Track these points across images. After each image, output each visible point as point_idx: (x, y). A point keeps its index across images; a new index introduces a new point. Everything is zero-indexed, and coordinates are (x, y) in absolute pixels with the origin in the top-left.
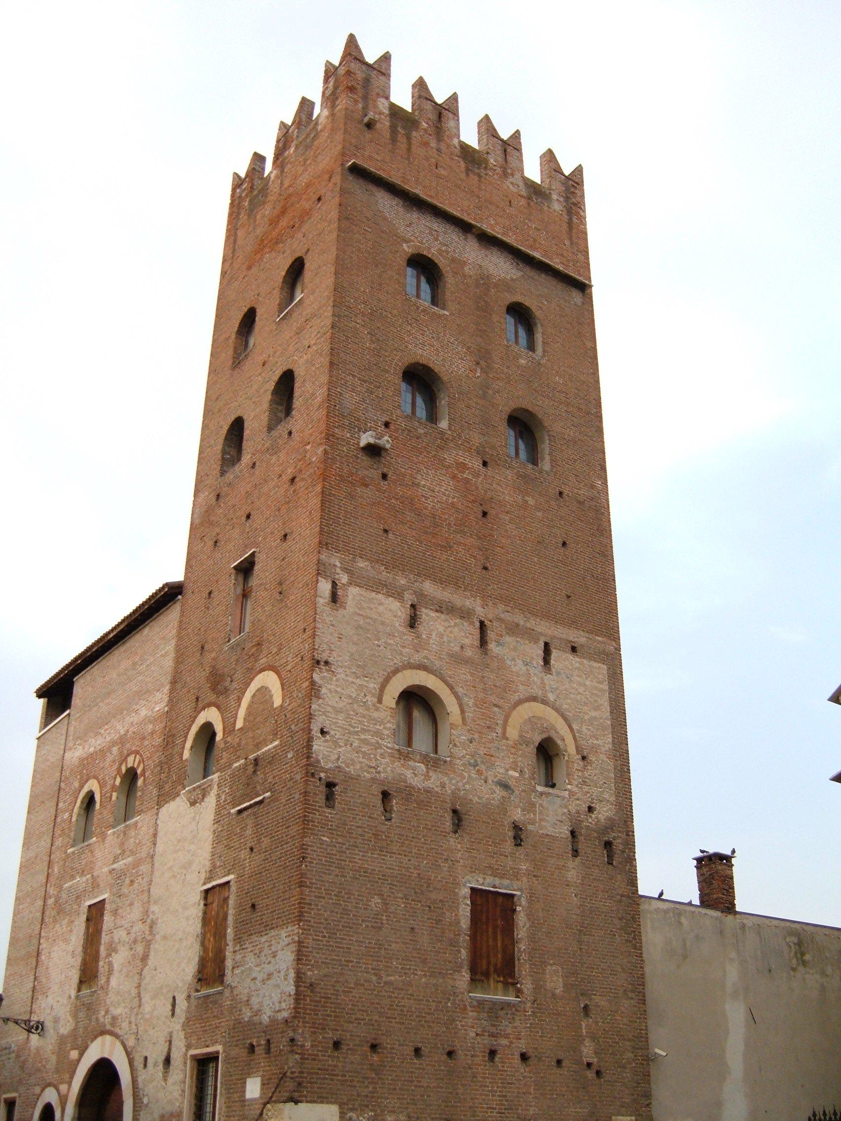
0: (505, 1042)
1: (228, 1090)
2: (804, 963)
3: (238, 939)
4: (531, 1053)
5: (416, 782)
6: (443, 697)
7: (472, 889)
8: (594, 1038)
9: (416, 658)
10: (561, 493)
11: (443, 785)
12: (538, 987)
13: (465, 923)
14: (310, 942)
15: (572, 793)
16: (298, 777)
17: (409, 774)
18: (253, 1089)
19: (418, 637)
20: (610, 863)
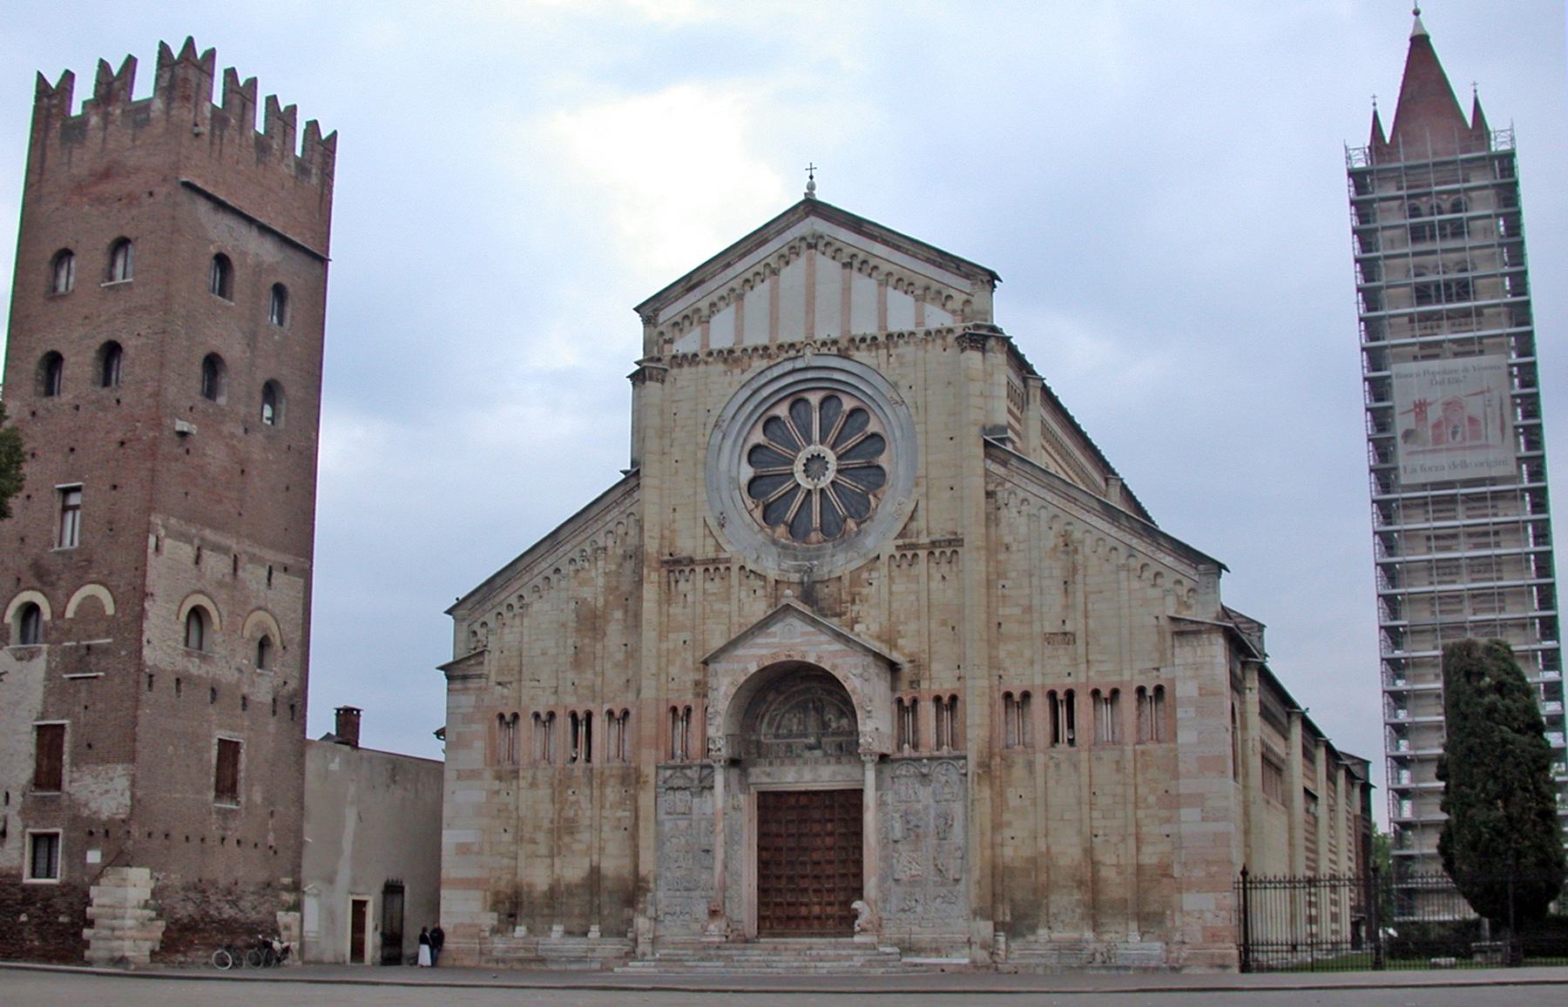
0: (229, 833)
1: (68, 853)
2: (395, 782)
3: (74, 763)
4: (243, 840)
5: (194, 671)
6: (209, 608)
7: (220, 740)
8: (275, 831)
9: (199, 586)
10: (289, 447)
11: (208, 673)
12: (249, 799)
13: (214, 761)
14: (139, 775)
15: (275, 673)
16: (132, 670)
17: (190, 666)
18: (94, 857)
19: (200, 570)
20: (292, 719)
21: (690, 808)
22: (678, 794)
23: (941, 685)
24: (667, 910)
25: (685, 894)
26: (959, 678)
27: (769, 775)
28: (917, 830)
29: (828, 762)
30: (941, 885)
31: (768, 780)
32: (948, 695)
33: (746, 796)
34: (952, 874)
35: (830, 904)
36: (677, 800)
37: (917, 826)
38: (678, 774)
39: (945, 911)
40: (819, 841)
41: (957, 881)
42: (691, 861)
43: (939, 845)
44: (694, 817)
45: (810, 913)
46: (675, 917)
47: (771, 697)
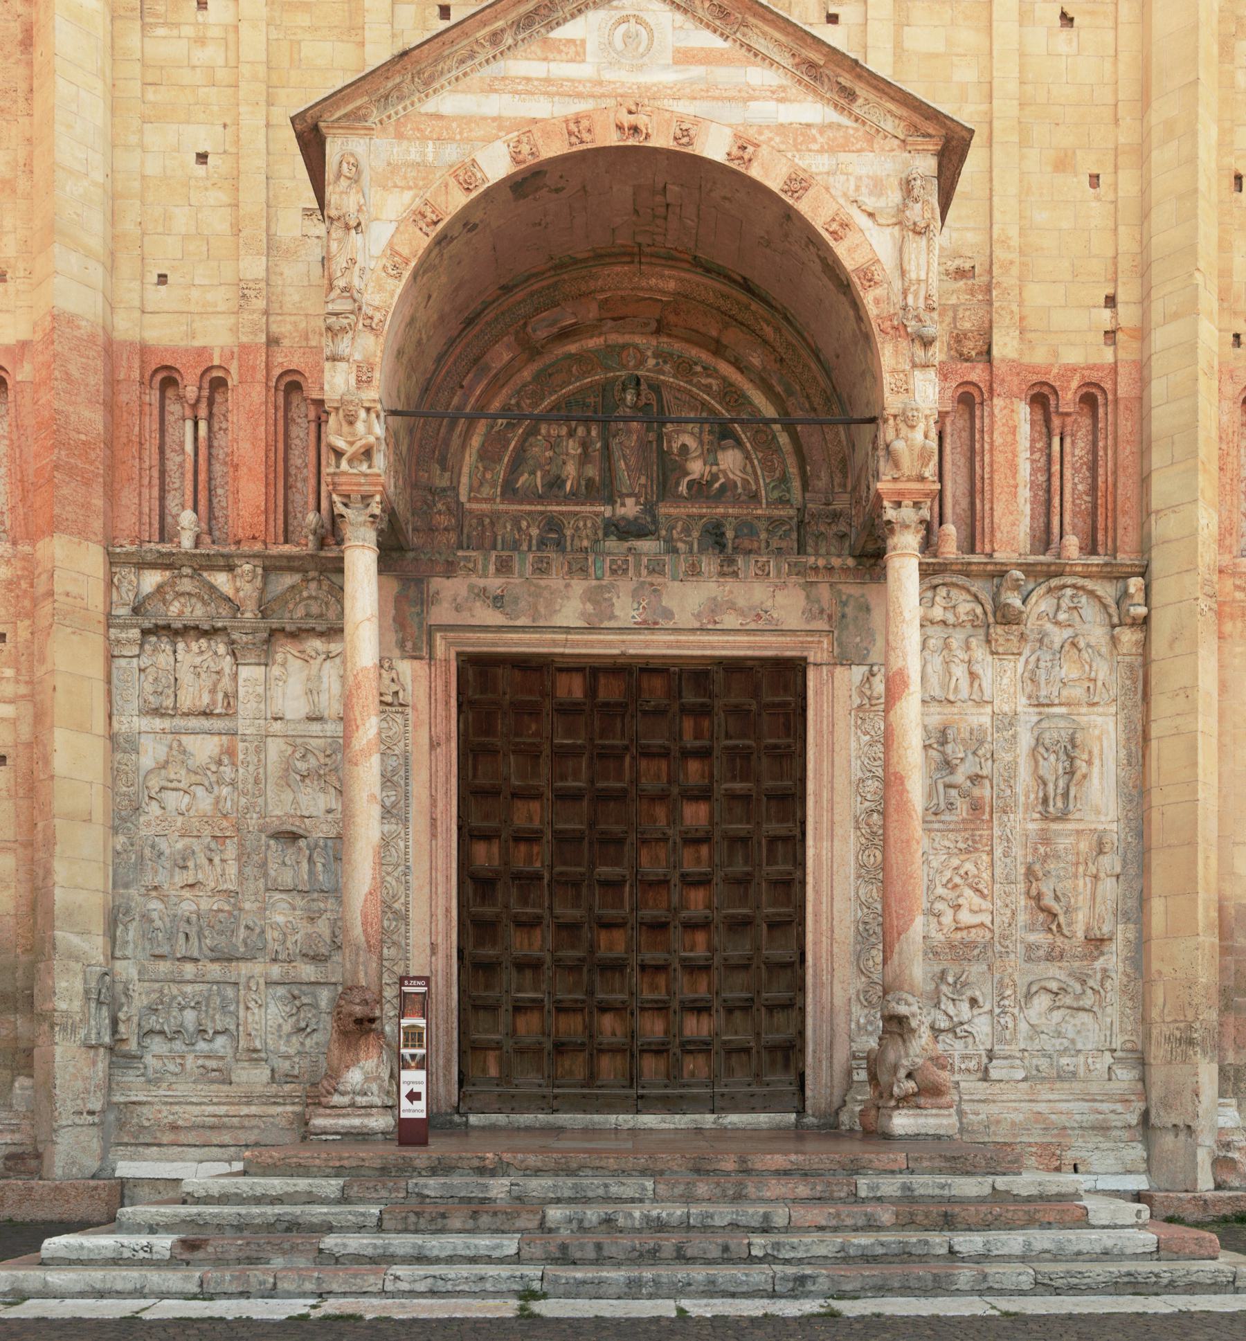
21: (230, 698)
22: (191, 653)
23: (1056, 354)
24: (153, 1022)
25: (215, 970)
26: (1110, 335)
27: (498, 601)
28: (976, 792)
29: (694, 572)
30: (1049, 958)
31: (493, 617)
32: (1074, 384)
33: (421, 667)
34: (1079, 924)
35: (700, 1008)
36: (186, 677)
37: (975, 779)
38: (186, 585)
39: (1059, 1034)
40: (660, 812)
41: (1097, 943)
42: (232, 869)
43: (1045, 838)
44: (244, 726)
45: (632, 1035)
46: (178, 1046)
47: (502, 355)
